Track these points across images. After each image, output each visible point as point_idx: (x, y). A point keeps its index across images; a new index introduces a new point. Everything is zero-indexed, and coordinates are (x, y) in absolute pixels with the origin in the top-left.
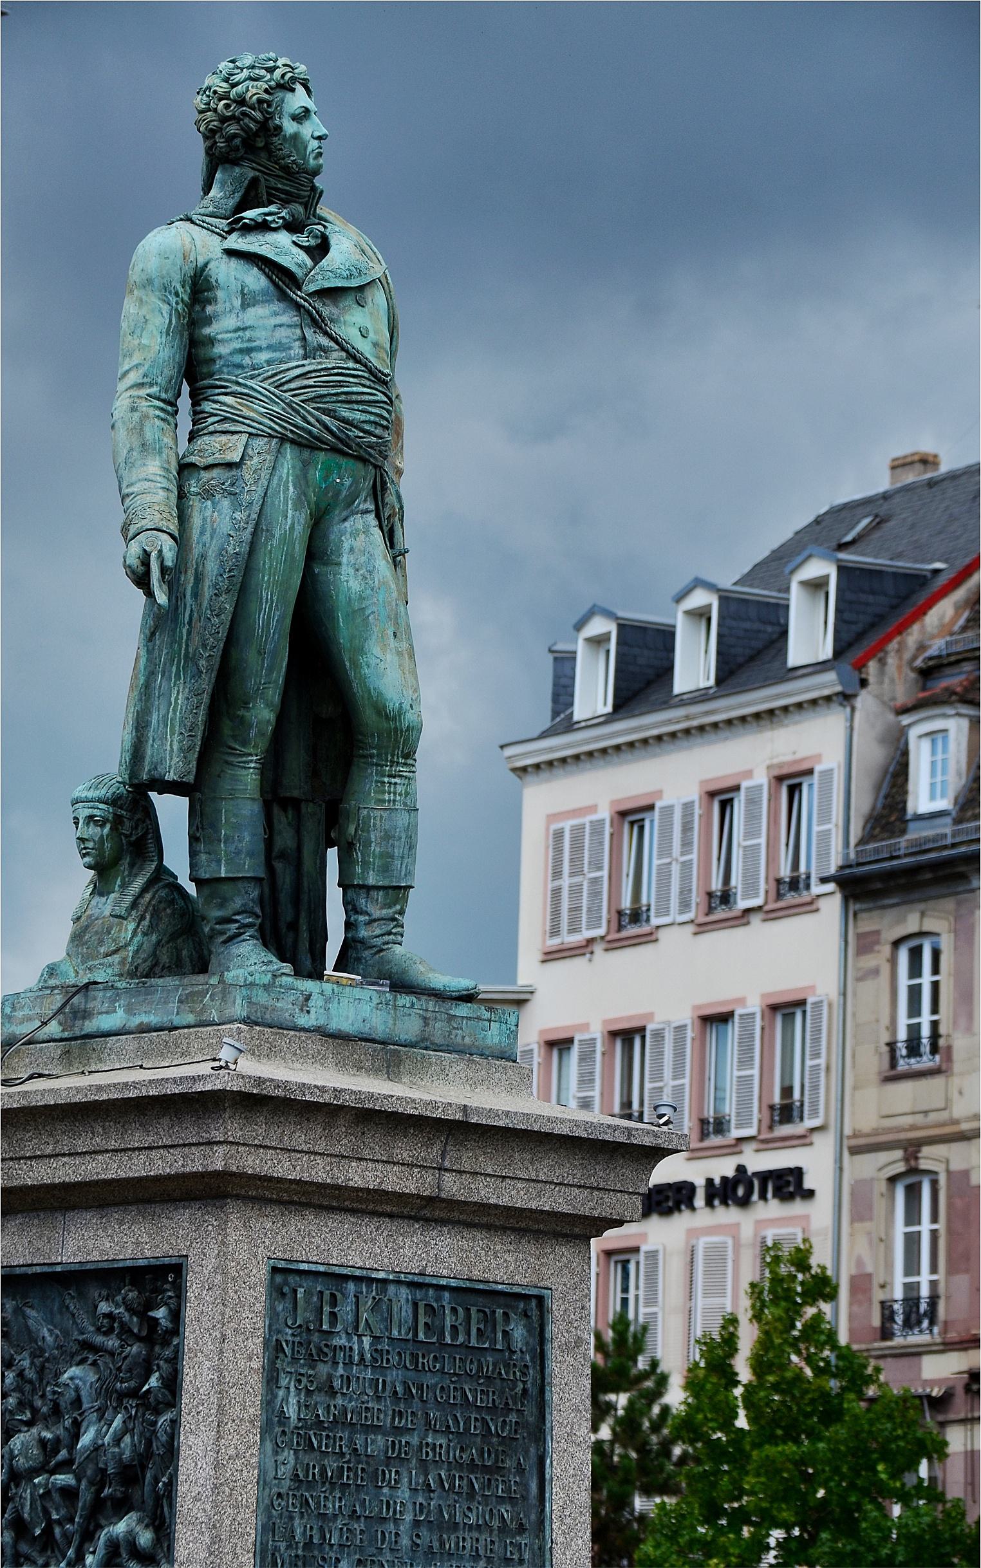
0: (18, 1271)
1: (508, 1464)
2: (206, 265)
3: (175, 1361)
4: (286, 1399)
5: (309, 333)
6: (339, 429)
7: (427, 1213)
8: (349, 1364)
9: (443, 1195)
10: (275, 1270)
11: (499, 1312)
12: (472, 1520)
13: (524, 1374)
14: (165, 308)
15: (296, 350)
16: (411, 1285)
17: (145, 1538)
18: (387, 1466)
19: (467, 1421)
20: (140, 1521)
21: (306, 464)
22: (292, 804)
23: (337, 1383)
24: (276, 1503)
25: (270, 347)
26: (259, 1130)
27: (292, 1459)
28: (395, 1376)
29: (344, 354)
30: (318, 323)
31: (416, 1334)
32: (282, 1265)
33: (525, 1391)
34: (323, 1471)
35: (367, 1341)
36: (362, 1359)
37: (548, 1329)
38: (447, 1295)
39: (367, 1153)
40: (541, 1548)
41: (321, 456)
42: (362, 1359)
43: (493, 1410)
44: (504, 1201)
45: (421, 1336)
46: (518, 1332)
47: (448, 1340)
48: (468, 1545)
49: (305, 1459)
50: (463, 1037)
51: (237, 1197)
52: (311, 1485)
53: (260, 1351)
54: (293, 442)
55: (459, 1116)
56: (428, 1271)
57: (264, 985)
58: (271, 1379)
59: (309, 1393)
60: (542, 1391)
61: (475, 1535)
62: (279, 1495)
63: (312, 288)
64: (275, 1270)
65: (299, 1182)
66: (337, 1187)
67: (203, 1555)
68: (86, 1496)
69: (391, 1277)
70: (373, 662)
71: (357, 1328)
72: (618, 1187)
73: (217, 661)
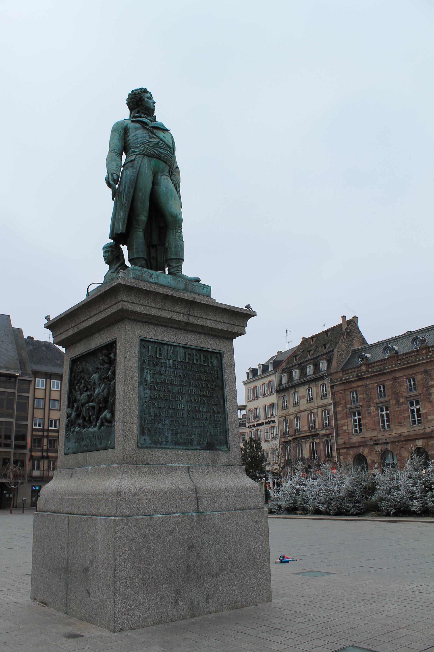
0: (84, 354)
1: (214, 396)
2: (127, 125)
3: (115, 367)
4: (147, 375)
5: (150, 134)
7: (186, 328)
8: (166, 367)
9: (190, 322)
10: (142, 340)
11: (209, 356)
12: (205, 410)
13: (217, 373)
14: (118, 135)
15: (148, 137)
16: (184, 347)
17: (109, 416)
18: (179, 395)
19: (202, 384)
20: (108, 412)
21: (150, 161)
22: (154, 246)
23: (162, 372)
24: (145, 404)
25: (141, 138)
26: (133, 299)
27: (149, 392)
28: (180, 372)
30: (152, 133)
31: (185, 360)
32: (143, 339)
33: (218, 377)
34: (159, 396)
35: (171, 361)
36: (170, 366)
37: (223, 361)
38: (194, 351)
39: (167, 308)
40: (225, 418)
42: (170, 366)
43: (209, 381)
44: (208, 325)
45: (187, 361)
46: (215, 362)
47: (195, 362)
48: (204, 417)
49: (154, 392)
51: (128, 319)
52: (156, 399)
53: (137, 361)
54: (147, 156)
55: (192, 299)
56: (188, 344)
58: (142, 370)
59: (154, 374)
60: (222, 377)
61: (206, 414)
62: (145, 402)
63: (151, 126)
64: (142, 340)
65: (146, 314)
66: (158, 317)
67: (122, 418)
68: (97, 408)
69: (177, 345)
70: (169, 205)
71: (168, 358)
72: (239, 325)
73: (130, 204)
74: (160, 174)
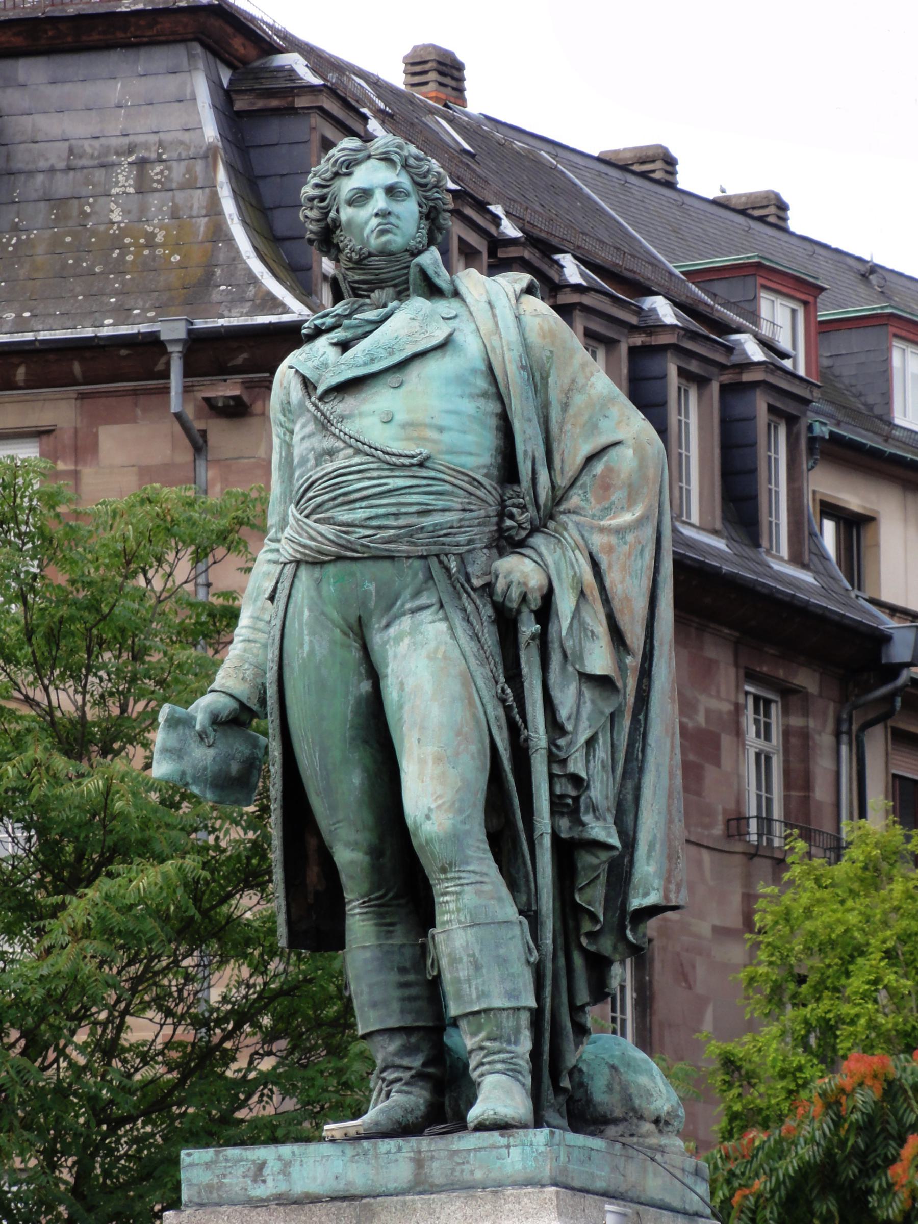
6: (337, 536)
21: (318, 582)
29: (350, 451)
41: (331, 569)
50: (472, 1172)
54: (307, 562)
57: (206, 1164)
74: (377, 624)
